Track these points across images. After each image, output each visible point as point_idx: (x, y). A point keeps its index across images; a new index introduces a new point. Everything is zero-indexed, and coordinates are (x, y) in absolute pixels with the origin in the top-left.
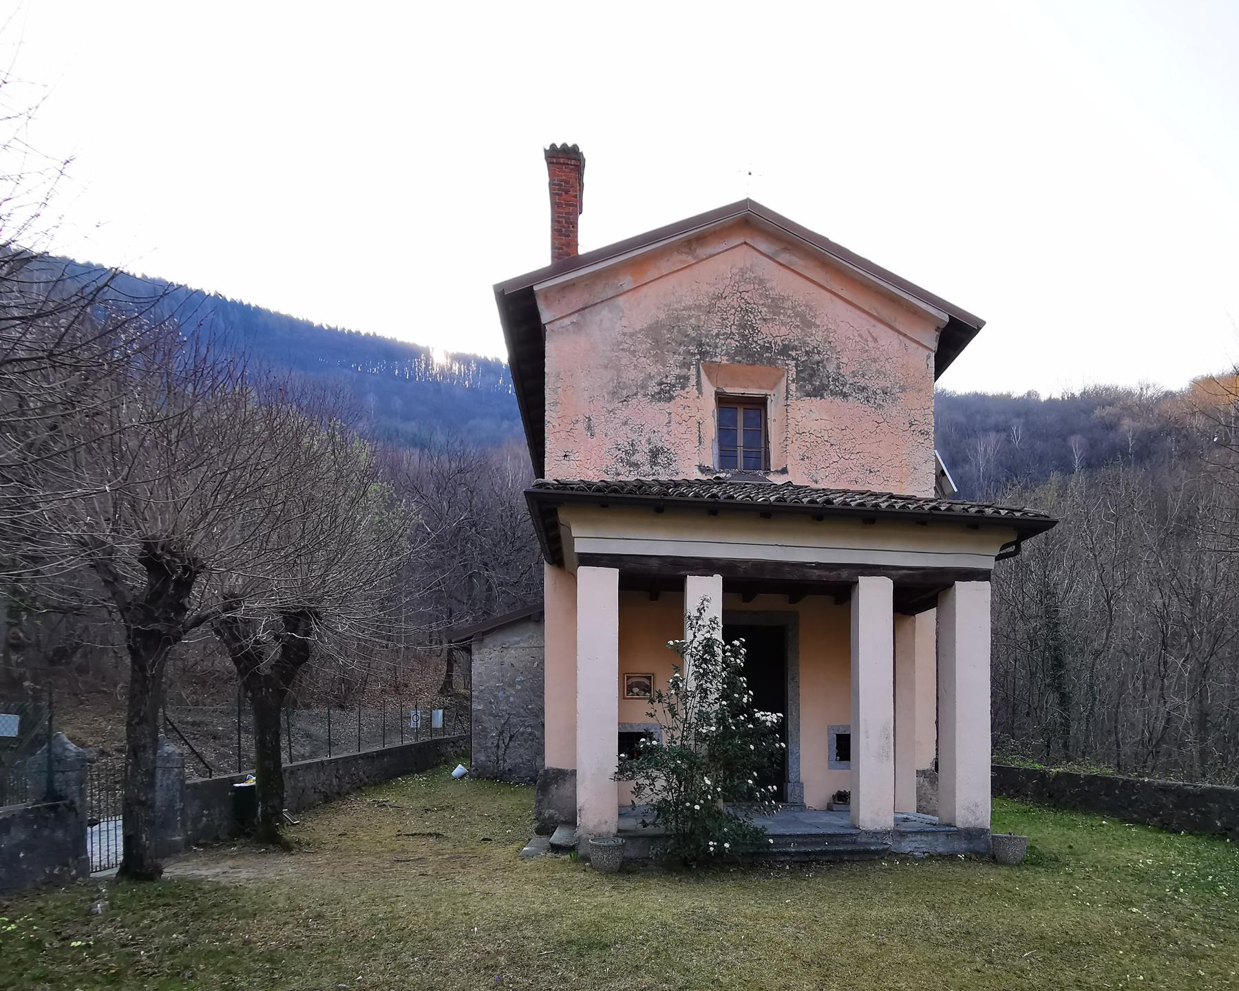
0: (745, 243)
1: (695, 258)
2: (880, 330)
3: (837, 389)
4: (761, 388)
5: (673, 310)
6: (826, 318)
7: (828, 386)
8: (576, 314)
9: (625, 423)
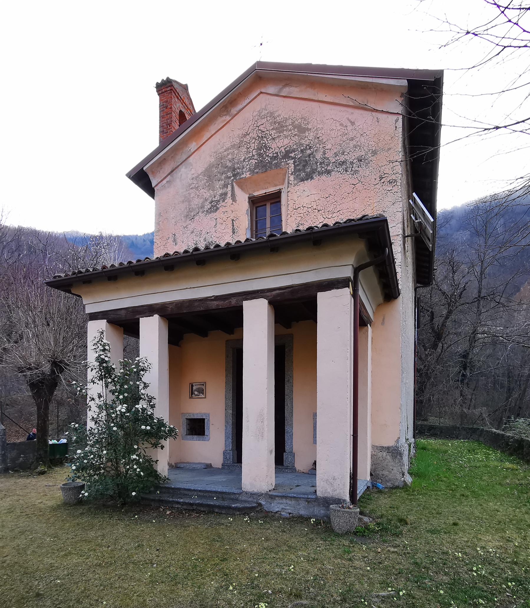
0: (261, 93)
1: (230, 116)
2: (357, 115)
3: (323, 169)
4: (276, 186)
5: (219, 154)
6: (316, 121)
7: (316, 170)
8: (169, 176)
9: (192, 232)
